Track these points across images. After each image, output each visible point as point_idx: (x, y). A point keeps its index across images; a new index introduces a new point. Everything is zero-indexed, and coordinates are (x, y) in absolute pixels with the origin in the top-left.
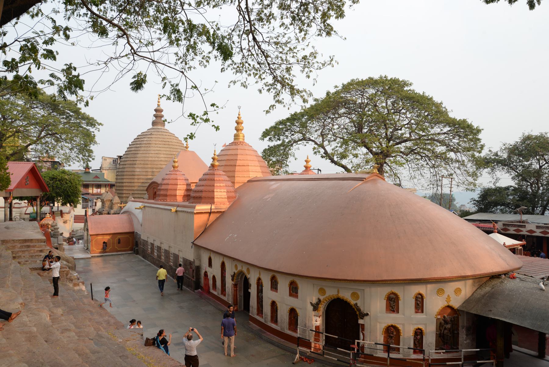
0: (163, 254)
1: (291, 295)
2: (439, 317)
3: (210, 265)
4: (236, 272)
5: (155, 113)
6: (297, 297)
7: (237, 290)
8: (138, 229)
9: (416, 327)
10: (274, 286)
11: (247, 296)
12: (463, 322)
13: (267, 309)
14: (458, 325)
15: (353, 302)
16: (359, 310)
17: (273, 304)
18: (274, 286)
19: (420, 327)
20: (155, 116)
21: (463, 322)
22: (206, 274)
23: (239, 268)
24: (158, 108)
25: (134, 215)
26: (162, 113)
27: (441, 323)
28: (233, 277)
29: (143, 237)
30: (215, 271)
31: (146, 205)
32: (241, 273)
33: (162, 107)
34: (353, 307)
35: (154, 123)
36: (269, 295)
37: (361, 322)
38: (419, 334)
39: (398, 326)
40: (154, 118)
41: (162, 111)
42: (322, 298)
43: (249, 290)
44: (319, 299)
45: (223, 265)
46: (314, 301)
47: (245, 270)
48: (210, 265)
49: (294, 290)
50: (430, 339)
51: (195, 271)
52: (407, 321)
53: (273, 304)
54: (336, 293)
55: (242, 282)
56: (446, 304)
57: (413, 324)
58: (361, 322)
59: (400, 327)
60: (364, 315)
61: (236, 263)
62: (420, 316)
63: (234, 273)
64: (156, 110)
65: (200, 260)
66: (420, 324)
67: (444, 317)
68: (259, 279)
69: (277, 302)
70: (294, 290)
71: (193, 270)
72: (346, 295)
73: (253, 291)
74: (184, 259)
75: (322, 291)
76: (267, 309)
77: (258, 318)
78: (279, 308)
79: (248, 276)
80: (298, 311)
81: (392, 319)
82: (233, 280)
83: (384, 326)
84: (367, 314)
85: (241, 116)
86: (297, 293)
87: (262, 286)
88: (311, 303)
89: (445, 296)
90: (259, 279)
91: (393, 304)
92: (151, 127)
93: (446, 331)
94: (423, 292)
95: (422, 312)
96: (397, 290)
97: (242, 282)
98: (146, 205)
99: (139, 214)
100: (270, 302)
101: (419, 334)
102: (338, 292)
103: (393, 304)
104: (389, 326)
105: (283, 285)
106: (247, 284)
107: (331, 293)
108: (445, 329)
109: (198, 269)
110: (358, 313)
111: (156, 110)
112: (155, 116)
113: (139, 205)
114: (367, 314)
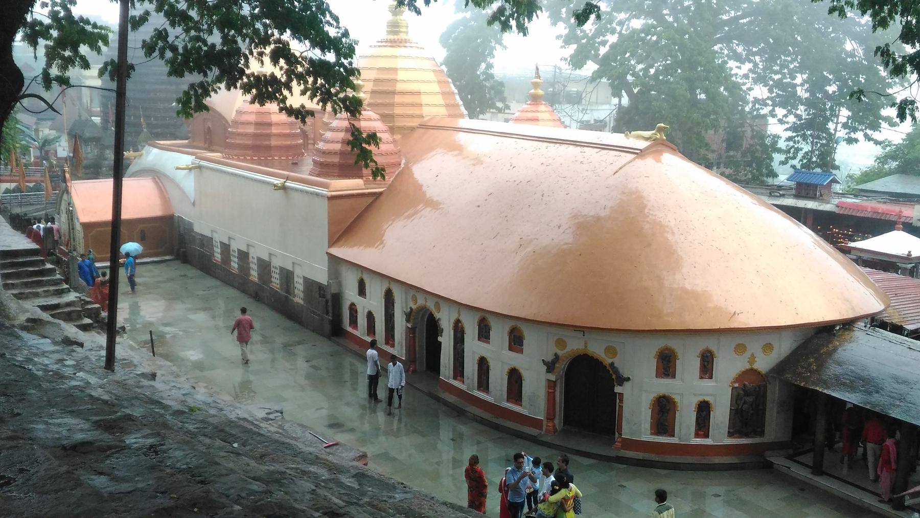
0: (255, 267)
1: (510, 349)
2: (736, 385)
3: (362, 292)
4: (414, 307)
6: (521, 351)
7: (414, 337)
8: (183, 211)
9: (701, 399)
10: (484, 333)
11: (434, 349)
12: (774, 394)
13: (471, 368)
14: (764, 396)
15: (607, 361)
16: (616, 371)
17: (483, 364)
18: (484, 333)
19: (707, 399)
21: (774, 394)
22: (353, 308)
23: (421, 301)
25: (172, 181)
27: (738, 395)
28: (409, 316)
29: (201, 227)
30: (374, 303)
31: (203, 163)
32: (423, 310)
34: (608, 367)
36: (473, 348)
37: (618, 389)
38: (704, 409)
39: (673, 396)
42: (560, 353)
43: (440, 339)
44: (556, 355)
45: (389, 298)
46: (550, 358)
47: (431, 305)
48: (362, 292)
49: (516, 341)
50: (721, 416)
51: (330, 304)
52: (688, 388)
53: (483, 364)
55: (426, 327)
56: (748, 366)
57: (695, 395)
58: (618, 389)
59: (677, 399)
60: (622, 380)
61: (413, 292)
62: (707, 383)
63: (411, 309)
65: (340, 285)
66: (707, 395)
67: (744, 385)
68: (458, 322)
69: (488, 360)
70: (516, 341)
71: (327, 302)
72: (597, 348)
73: (446, 340)
74: (306, 280)
75: (561, 343)
76: (471, 368)
77: (457, 383)
78: (491, 367)
79: (437, 315)
80: (522, 372)
81: (664, 386)
82: (408, 321)
83: (652, 396)
84: (628, 379)
86: (521, 345)
87: (463, 333)
89: (748, 354)
90: (458, 322)
91: (666, 364)
93: (745, 406)
94: (713, 347)
95: (711, 377)
96: (674, 344)
97: (426, 327)
98: (203, 163)
99: (188, 183)
101: (704, 409)
102: (586, 344)
103: (666, 364)
104: (660, 397)
105: (499, 334)
106: (433, 327)
107: (575, 345)
108: (745, 403)
109: (337, 299)
110: (614, 377)
113: (187, 160)
114: (628, 379)
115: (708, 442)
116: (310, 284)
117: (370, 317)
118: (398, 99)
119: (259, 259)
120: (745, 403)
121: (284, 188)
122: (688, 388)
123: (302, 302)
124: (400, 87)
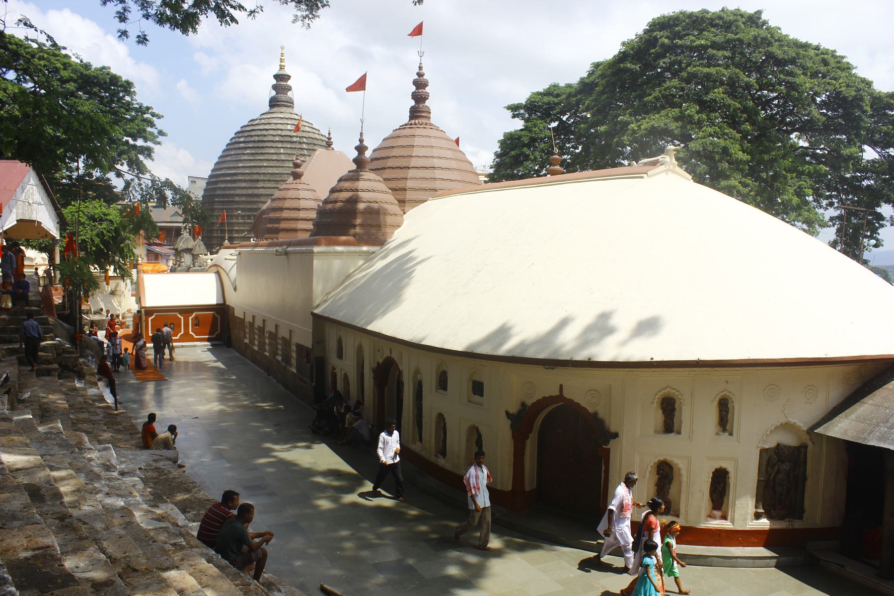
5: (274, 82)
10: (442, 383)
17: (441, 417)
19: (724, 465)
20: (275, 87)
24: (282, 72)
26: (289, 83)
33: (287, 71)
35: (274, 103)
40: (274, 93)
41: (289, 77)
52: (698, 451)
64: (276, 77)
81: (668, 448)
85: (424, 71)
90: (417, 372)
92: (267, 109)
100: (434, 416)
111: (276, 77)
112: (275, 87)
114: (616, 435)
115: (726, 525)
116: (300, 347)
117: (346, 376)
118: (411, 173)
119: (270, 333)
120: (778, 472)
121: (286, 253)
122: (698, 451)
123: (295, 371)
124: (414, 162)
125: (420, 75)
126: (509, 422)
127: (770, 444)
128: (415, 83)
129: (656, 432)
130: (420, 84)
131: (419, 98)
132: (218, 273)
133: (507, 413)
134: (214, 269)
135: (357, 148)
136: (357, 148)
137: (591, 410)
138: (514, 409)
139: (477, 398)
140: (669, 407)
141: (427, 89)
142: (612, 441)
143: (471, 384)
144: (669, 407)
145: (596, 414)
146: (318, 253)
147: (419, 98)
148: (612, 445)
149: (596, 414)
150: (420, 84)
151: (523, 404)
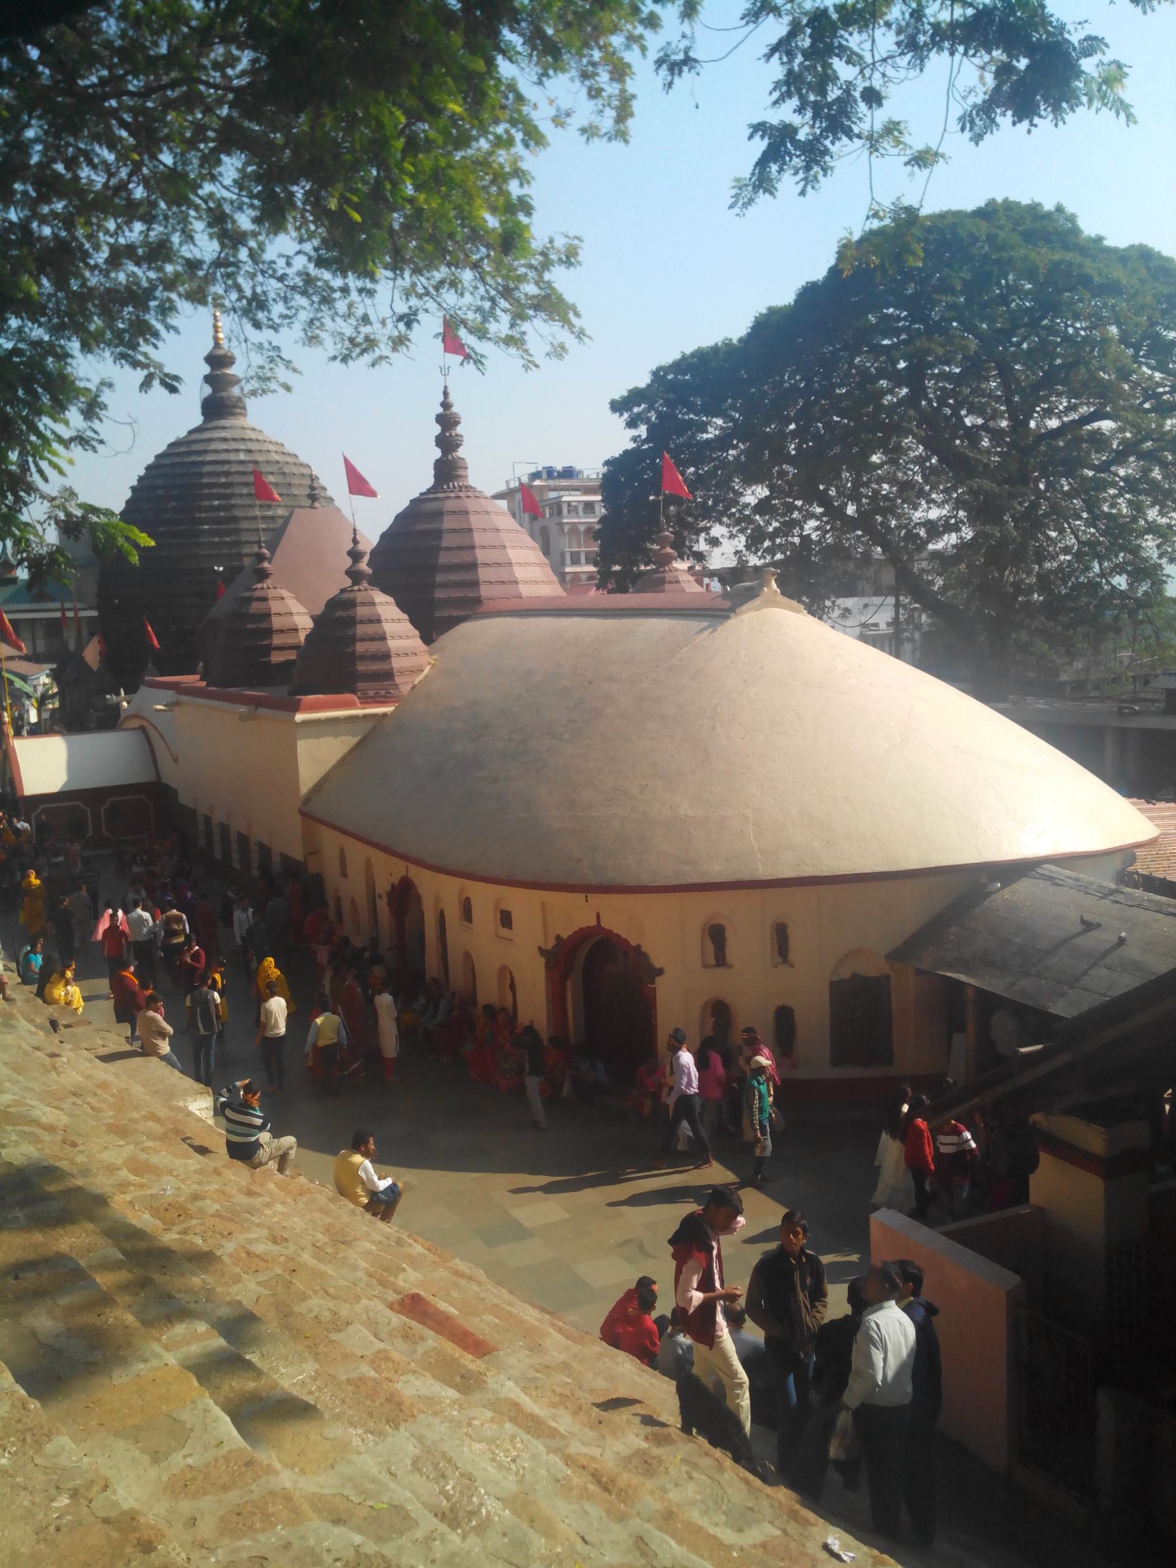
20: (208, 379)
54: (593, 923)
85: (451, 399)
88: (540, 948)
125: (446, 405)
126: (543, 960)
127: (845, 973)
128: (440, 419)
129: (705, 966)
130: (447, 420)
131: (447, 442)
132: (142, 729)
133: (540, 948)
134: (135, 723)
135: (350, 553)
136: (350, 553)
137: (634, 943)
138: (550, 944)
139: (505, 932)
140: (716, 935)
141: (459, 429)
142: (658, 980)
143: (499, 915)
144: (716, 935)
145: (638, 947)
146: (305, 723)
147: (447, 442)
148: (659, 981)
149: (638, 947)
150: (447, 420)
151: (558, 938)
